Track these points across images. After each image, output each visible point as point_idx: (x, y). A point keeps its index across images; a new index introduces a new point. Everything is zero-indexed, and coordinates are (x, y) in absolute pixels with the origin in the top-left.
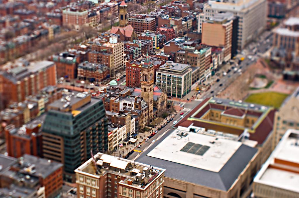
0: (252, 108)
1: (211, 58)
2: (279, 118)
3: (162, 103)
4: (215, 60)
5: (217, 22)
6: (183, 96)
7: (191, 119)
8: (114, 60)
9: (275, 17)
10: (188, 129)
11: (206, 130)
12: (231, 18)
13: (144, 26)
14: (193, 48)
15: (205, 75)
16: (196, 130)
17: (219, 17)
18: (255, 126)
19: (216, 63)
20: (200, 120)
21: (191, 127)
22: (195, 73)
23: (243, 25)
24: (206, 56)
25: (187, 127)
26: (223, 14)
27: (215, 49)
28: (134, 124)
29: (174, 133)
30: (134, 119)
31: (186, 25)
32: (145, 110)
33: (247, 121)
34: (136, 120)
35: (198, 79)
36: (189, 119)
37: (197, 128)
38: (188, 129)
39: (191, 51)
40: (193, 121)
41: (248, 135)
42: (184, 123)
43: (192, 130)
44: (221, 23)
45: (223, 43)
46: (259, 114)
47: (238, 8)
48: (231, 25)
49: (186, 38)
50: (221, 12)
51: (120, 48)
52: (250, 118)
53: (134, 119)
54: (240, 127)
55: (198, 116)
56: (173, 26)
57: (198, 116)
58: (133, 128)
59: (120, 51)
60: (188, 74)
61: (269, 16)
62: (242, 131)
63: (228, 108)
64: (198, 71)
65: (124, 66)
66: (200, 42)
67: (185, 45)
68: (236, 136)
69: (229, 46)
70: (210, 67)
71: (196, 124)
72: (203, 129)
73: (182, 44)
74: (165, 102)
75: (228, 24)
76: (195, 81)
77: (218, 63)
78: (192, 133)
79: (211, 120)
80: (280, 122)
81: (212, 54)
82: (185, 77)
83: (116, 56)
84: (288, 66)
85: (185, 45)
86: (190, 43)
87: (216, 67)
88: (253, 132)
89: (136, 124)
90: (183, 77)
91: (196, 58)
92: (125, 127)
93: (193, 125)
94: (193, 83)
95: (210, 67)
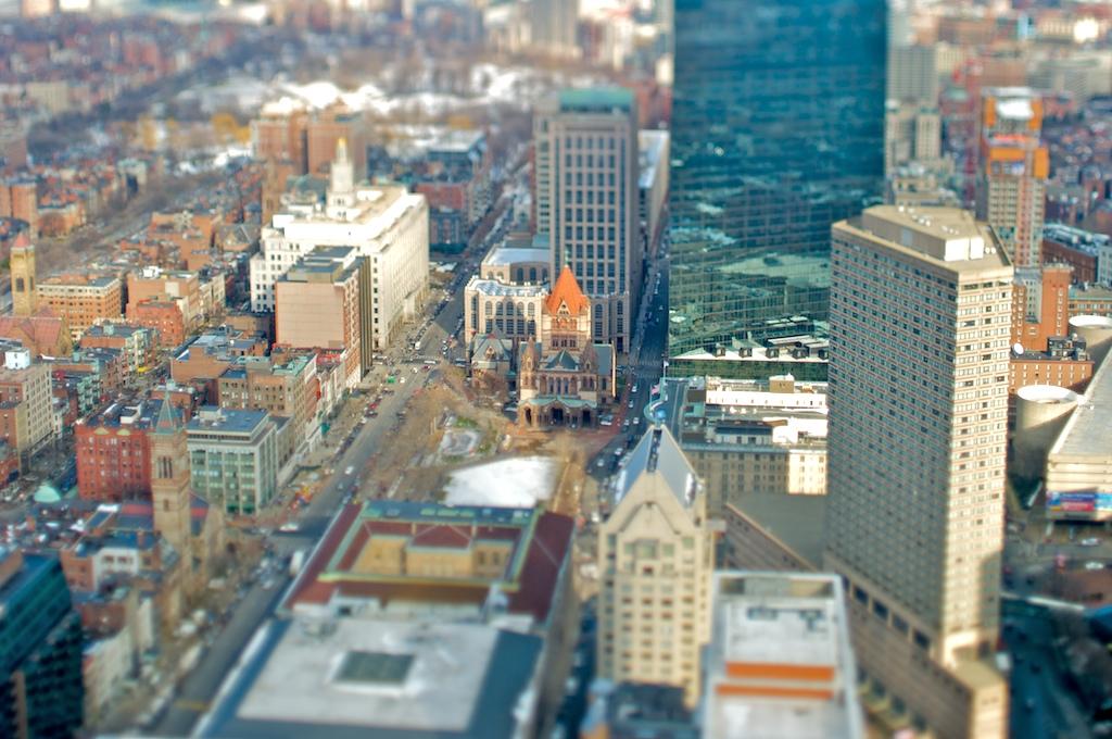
3: (213, 541)
4: (327, 387)
8: (27, 420)
11: (384, 604)
13: (88, 306)
15: (307, 437)
16: (354, 610)
19: (329, 397)
24: (306, 379)
27: (326, 358)
29: (294, 633)
31: (210, 293)
35: (291, 452)
37: (354, 602)
41: (503, 600)
43: (345, 611)
48: (356, 283)
51: (41, 383)
56: (174, 299)
57: (347, 564)
58: (147, 634)
59: (42, 391)
60: (268, 440)
65: (56, 435)
68: (471, 610)
69: (355, 343)
70: (317, 412)
71: (349, 588)
72: (374, 604)
75: (349, 280)
76: (286, 458)
77: (334, 398)
78: (346, 622)
82: (262, 447)
83: (32, 408)
87: (329, 409)
90: (255, 449)
91: (281, 388)
94: (281, 465)
95: (317, 412)
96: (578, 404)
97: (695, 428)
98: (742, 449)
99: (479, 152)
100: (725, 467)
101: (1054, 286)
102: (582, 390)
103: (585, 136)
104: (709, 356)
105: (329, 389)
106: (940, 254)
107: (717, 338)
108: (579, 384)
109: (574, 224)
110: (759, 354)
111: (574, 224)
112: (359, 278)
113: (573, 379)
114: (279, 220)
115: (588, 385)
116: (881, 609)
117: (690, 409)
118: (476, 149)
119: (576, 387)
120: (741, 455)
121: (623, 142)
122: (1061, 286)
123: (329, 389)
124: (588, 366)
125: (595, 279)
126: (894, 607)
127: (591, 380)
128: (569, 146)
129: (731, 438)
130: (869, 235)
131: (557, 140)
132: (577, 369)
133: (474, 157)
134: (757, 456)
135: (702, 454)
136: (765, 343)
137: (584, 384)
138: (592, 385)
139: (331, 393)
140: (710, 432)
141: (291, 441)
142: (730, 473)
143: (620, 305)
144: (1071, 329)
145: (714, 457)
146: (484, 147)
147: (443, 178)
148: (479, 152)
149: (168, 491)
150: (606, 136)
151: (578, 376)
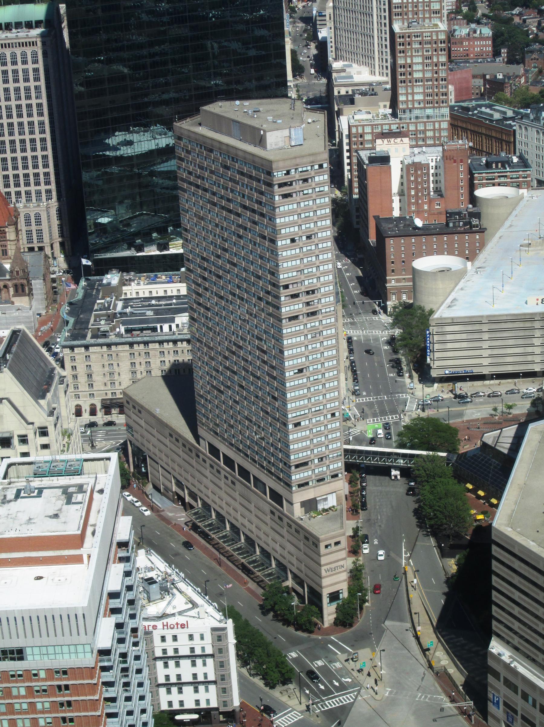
101: (455, 162)
102: (14, 296)
103: (18, 51)
106: (261, 142)
107: (137, 234)
113: (5, 286)
116: (244, 473)
119: (9, 294)
122: (461, 161)
124: (17, 272)
125: (33, 188)
126: (254, 470)
127: (22, 285)
130: (202, 130)
132: (8, 277)
137: (16, 290)
138: (23, 290)
142: (137, 360)
144: (473, 200)
145: (120, 348)
151: (10, 284)
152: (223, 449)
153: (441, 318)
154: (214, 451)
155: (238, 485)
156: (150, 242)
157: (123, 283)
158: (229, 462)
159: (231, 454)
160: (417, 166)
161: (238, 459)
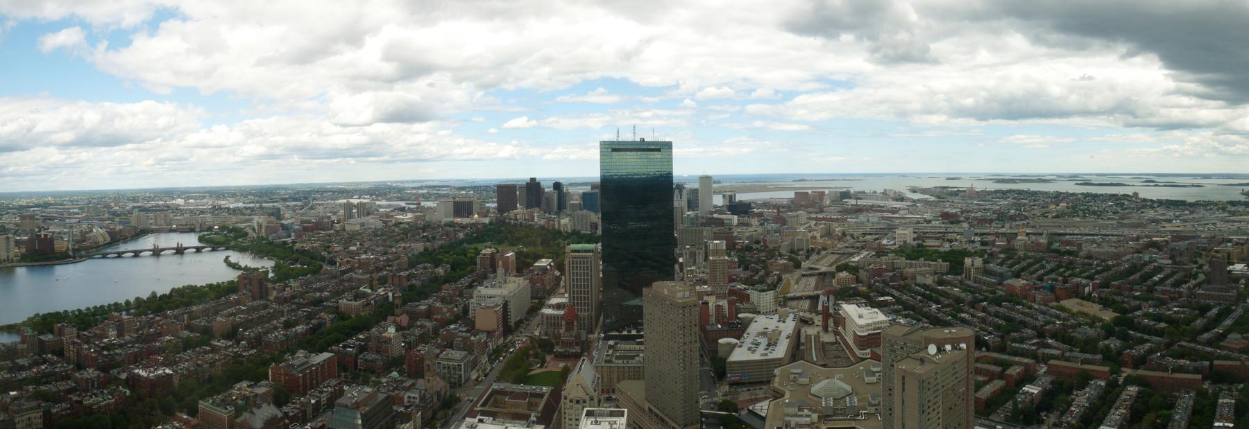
0: (534, 390)
1: (486, 343)
2: (566, 398)
5: (488, 307)
6: (464, 384)
7: (478, 409)
9: (536, 299)
10: (476, 420)
11: (494, 420)
12: (500, 301)
14: (469, 334)
17: (490, 303)
18: (540, 408)
20: (486, 408)
21: (479, 417)
22: (473, 360)
23: (512, 308)
25: (475, 418)
26: (492, 299)
27: (489, 333)
28: (420, 419)
30: (420, 413)
32: (430, 402)
33: (530, 404)
34: (422, 414)
35: (476, 366)
36: (475, 409)
37: (485, 418)
38: (476, 420)
39: (468, 338)
40: (481, 411)
41: (535, 419)
42: (472, 414)
43: (481, 421)
44: (493, 308)
45: (496, 327)
46: (541, 396)
47: (505, 292)
49: (460, 326)
50: (490, 297)
52: (534, 400)
53: (420, 413)
54: (526, 411)
55: (484, 405)
61: (532, 298)
62: (530, 416)
63: (511, 393)
64: (476, 357)
66: (473, 327)
67: (461, 331)
69: (501, 329)
71: (484, 413)
72: (491, 418)
73: (457, 331)
74: (448, 393)
75: (499, 308)
76: (474, 368)
78: (480, 425)
79: (496, 407)
80: (568, 401)
81: (487, 339)
84: (557, 344)
85: (461, 331)
86: (465, 329)
87: (491, 351)
88: (539, 415)
89: (422, 419)
92: (411, 422)
93: (481, 415)
94: (472, 370)
96: (574, 351)
97: (608, 358)
98: (624, 365)
99: (551, 266)
100: (618, 372)
103: (578, 260)
104: (617, 333)
105: (491, 345)
108: (574, 344)
109: (576, 289)
110: (634, 332)
111: (576, 289)
112: (503, 307)
114: (479, 288)
115: (577, 344)
116: (662, 420)
117: (608, 352)
118: (550, 265)
120: (624, 367)
121: (591, 261)
123: (491, 345)
126: (666, 419)
128: (573, 263)
129: (620, 361)
131: (569, 261)
133: (548, 267)
134: (629, 367)
135: (610, 367)
136: (636, 328)
139: (491, 346)
140: (614, 359)
141: (476, 362)
143: (591, 317)
146: (552, 264)
147: (537, 274)
148: (551, 266)
149: (429, 376)
150: (585, 260)
152: (655, 410)
153: (730, 362)
154: (650, 409)
155: (660, 425)
156: (624, 329)
157: (616, 344)
158: (657, 415)
159: (657, 412)
160: (719, 306)
161: (660, 414)
